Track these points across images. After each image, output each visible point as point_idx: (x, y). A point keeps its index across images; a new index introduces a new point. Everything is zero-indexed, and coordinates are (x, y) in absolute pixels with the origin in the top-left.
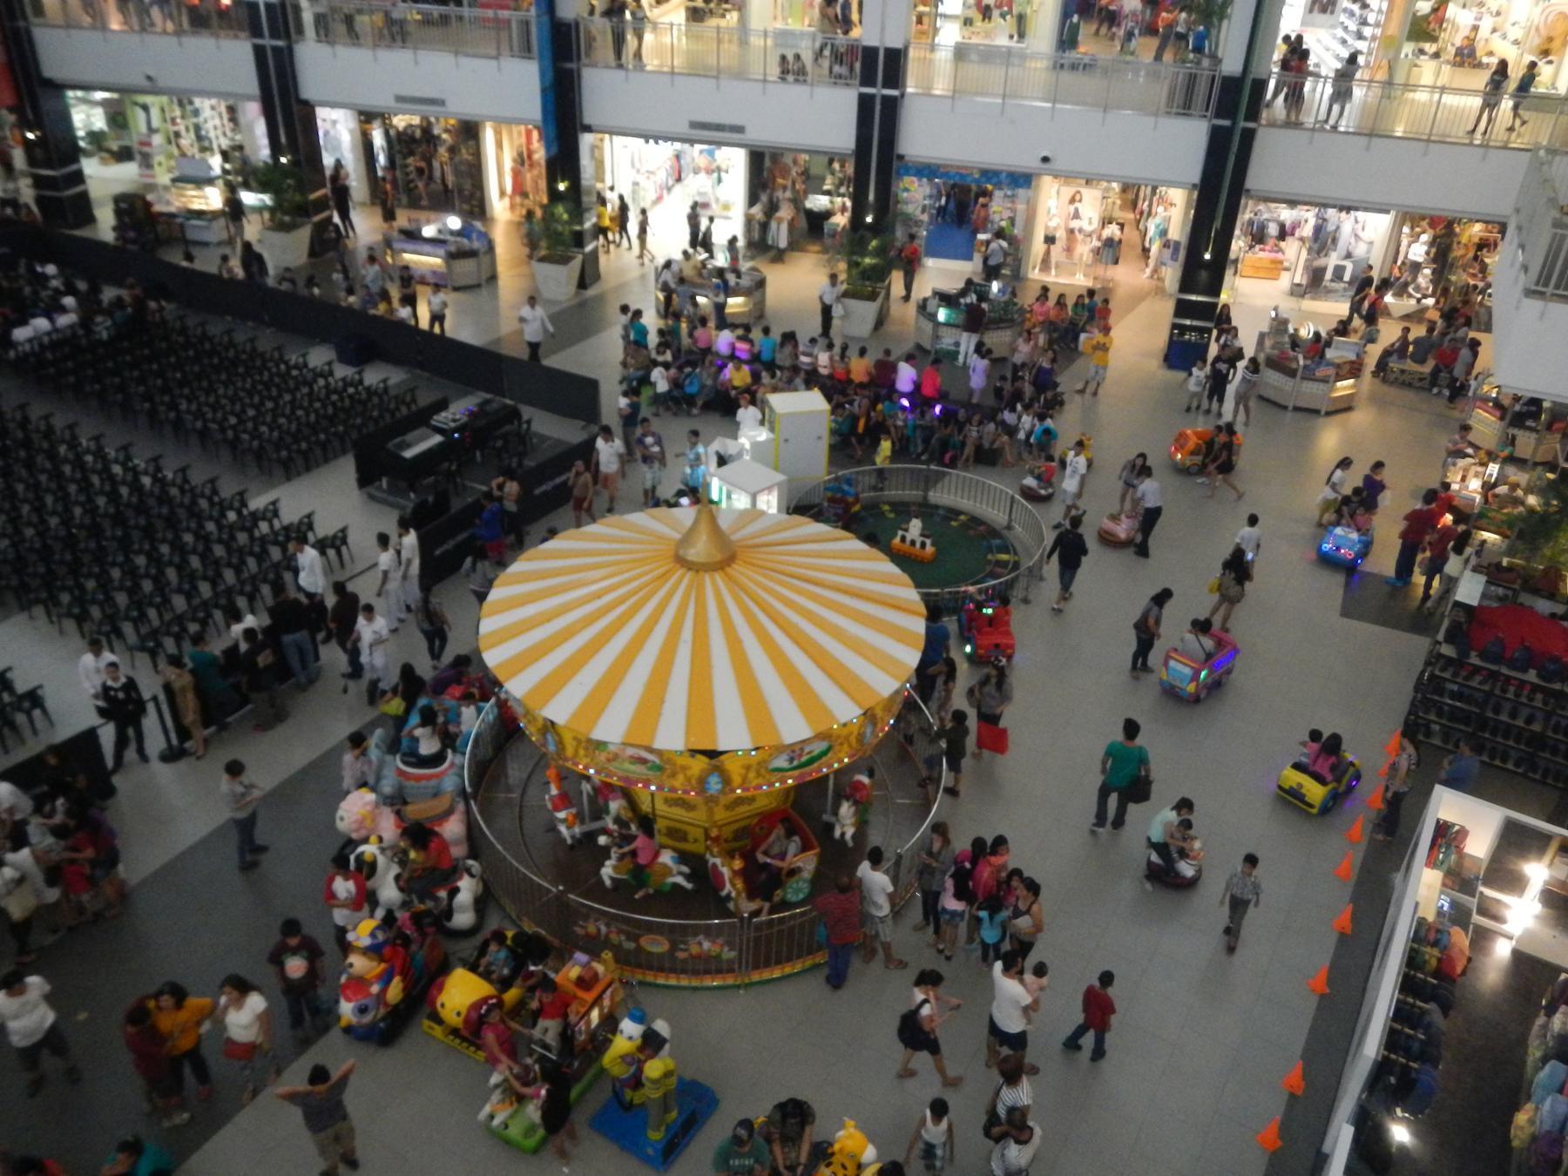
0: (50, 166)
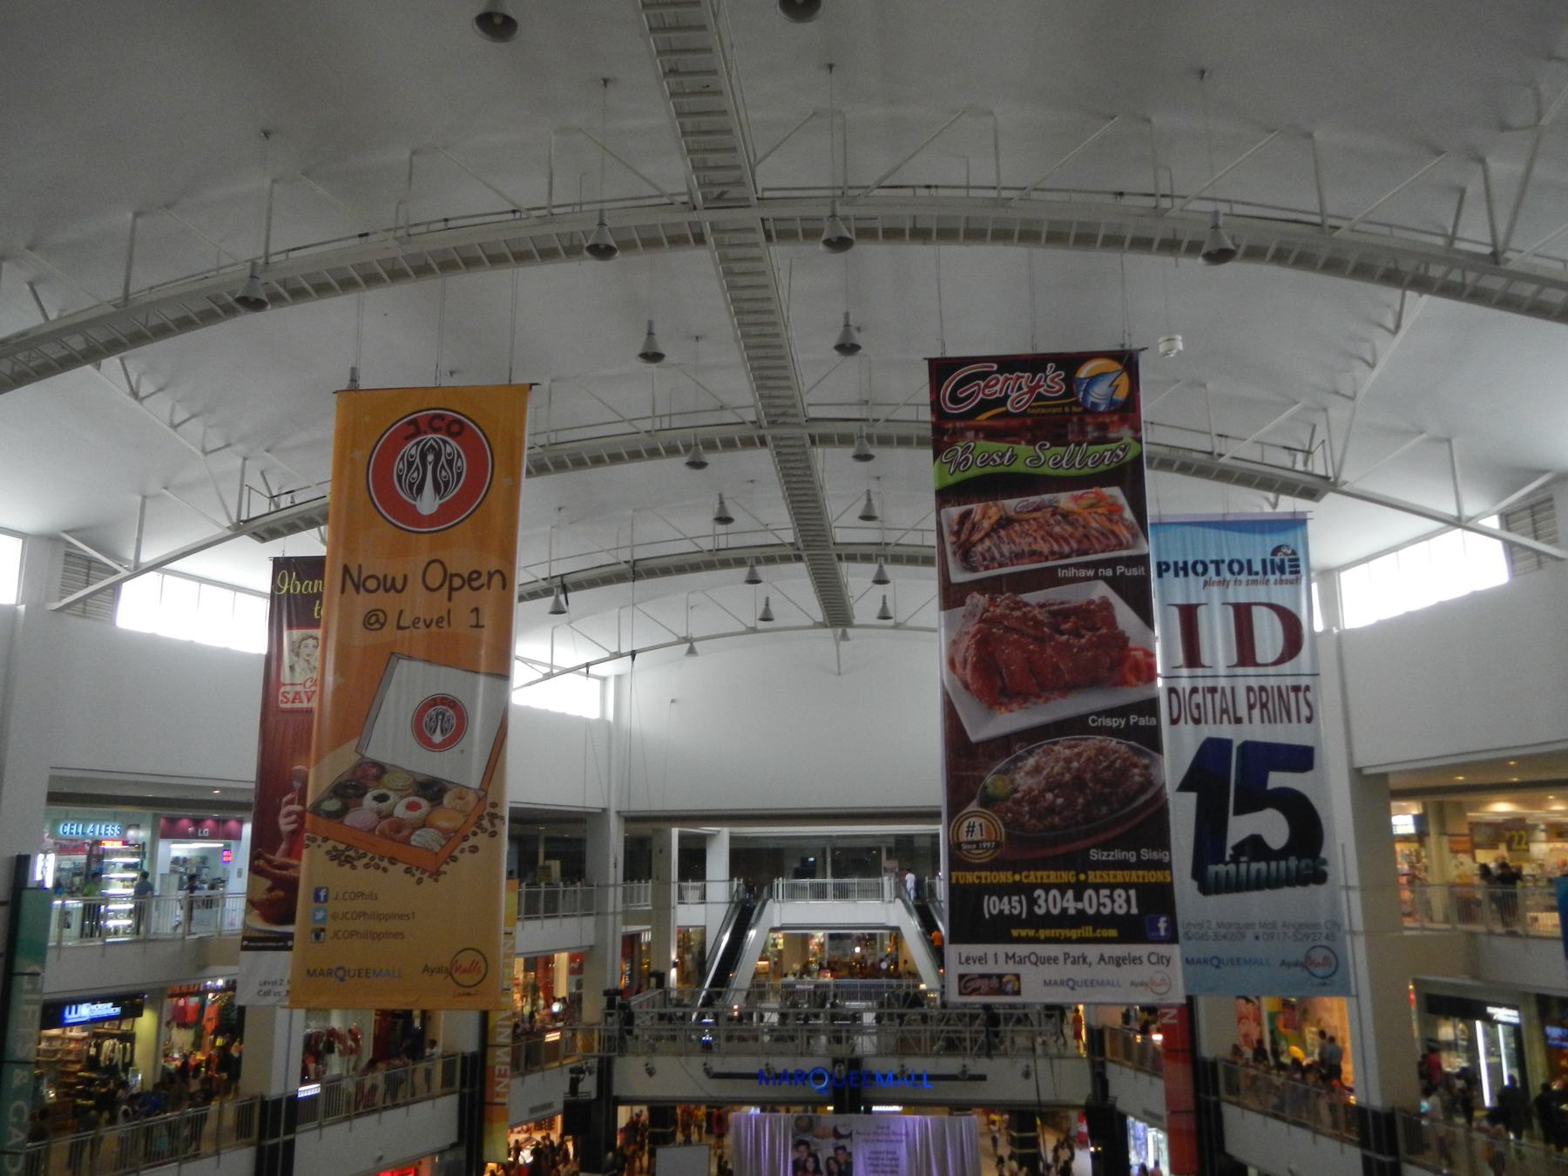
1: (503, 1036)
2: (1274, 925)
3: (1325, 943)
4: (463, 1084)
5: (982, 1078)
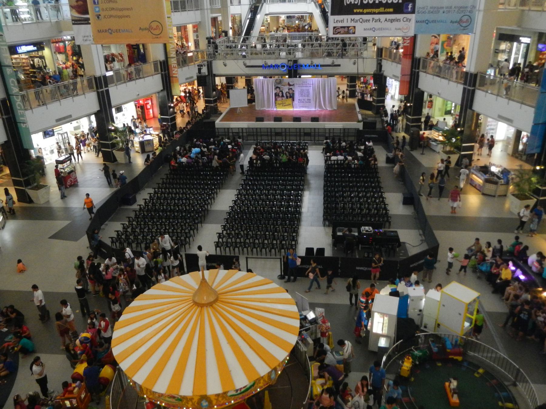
0: (410, 115)
1: (173, 54)
2: (451, 7)
3: (468, 14)
4: (162, 71)
5: (339, 65)
